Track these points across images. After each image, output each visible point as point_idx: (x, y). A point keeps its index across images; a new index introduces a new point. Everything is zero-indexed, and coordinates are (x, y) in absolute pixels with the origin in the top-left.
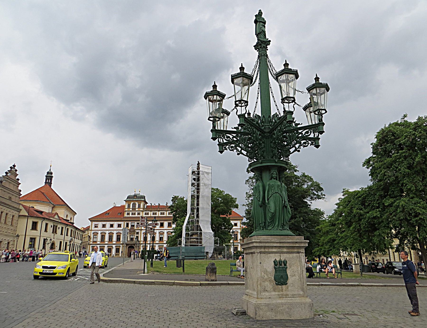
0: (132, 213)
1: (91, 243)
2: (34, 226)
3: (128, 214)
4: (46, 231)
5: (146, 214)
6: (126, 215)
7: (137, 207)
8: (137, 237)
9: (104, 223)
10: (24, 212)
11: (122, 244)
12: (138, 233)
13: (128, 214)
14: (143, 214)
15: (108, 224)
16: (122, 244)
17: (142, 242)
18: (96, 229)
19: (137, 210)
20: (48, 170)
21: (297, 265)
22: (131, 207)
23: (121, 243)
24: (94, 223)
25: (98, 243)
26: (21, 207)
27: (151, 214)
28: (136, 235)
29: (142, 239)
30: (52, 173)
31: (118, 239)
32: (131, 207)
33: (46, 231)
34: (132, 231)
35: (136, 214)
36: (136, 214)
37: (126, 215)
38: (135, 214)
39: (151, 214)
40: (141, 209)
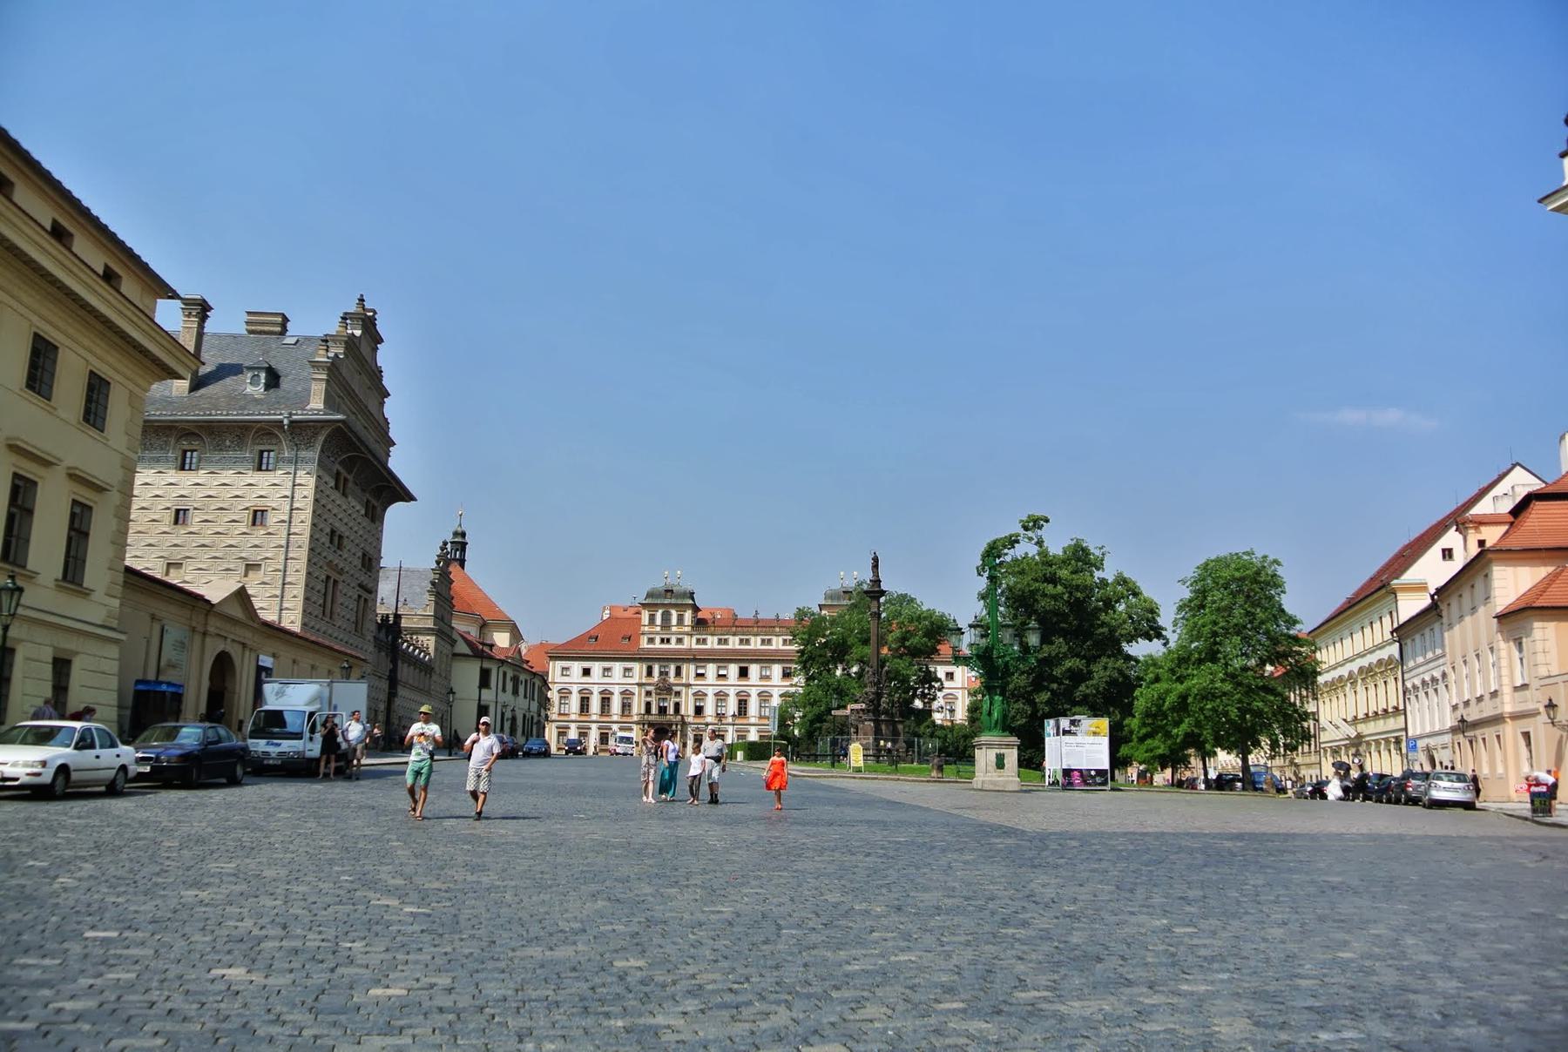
0: (662, 641)
1: (554, 717)
2: (484, 682)
3: (651, 641)
4: (504, 690)
5: (698, 641)
6: (644, 644)
7: (674, 621)
8: (677, 706)
9: (586, 664)
10: (462, 648)
11: (637, 723)
12: (678, 694)
13: (651, 641)
14: (690, 643)
15: (597, 667)
16: (637, 723)
17: (690, 720)
18: (566, 679)
19: (674, 629)
20: (455, 527)
21: (1012, 756)
22: (658, 621)
23: (635, 718)
24: (559, 664)
25: (573, 717)
26: (455, 636)
27: (712, 642)
28: (674, 699)
29: (691, 711)
30: (463, 535)
31: (626, 706)
32: (658, 621)
33: (504, 690)
34: (665, 689)
35: (673, 640)
36: (673, 640)
37: (644, 644)
38: (668, 641)
39: (712, 642)
40: (687, 629)
